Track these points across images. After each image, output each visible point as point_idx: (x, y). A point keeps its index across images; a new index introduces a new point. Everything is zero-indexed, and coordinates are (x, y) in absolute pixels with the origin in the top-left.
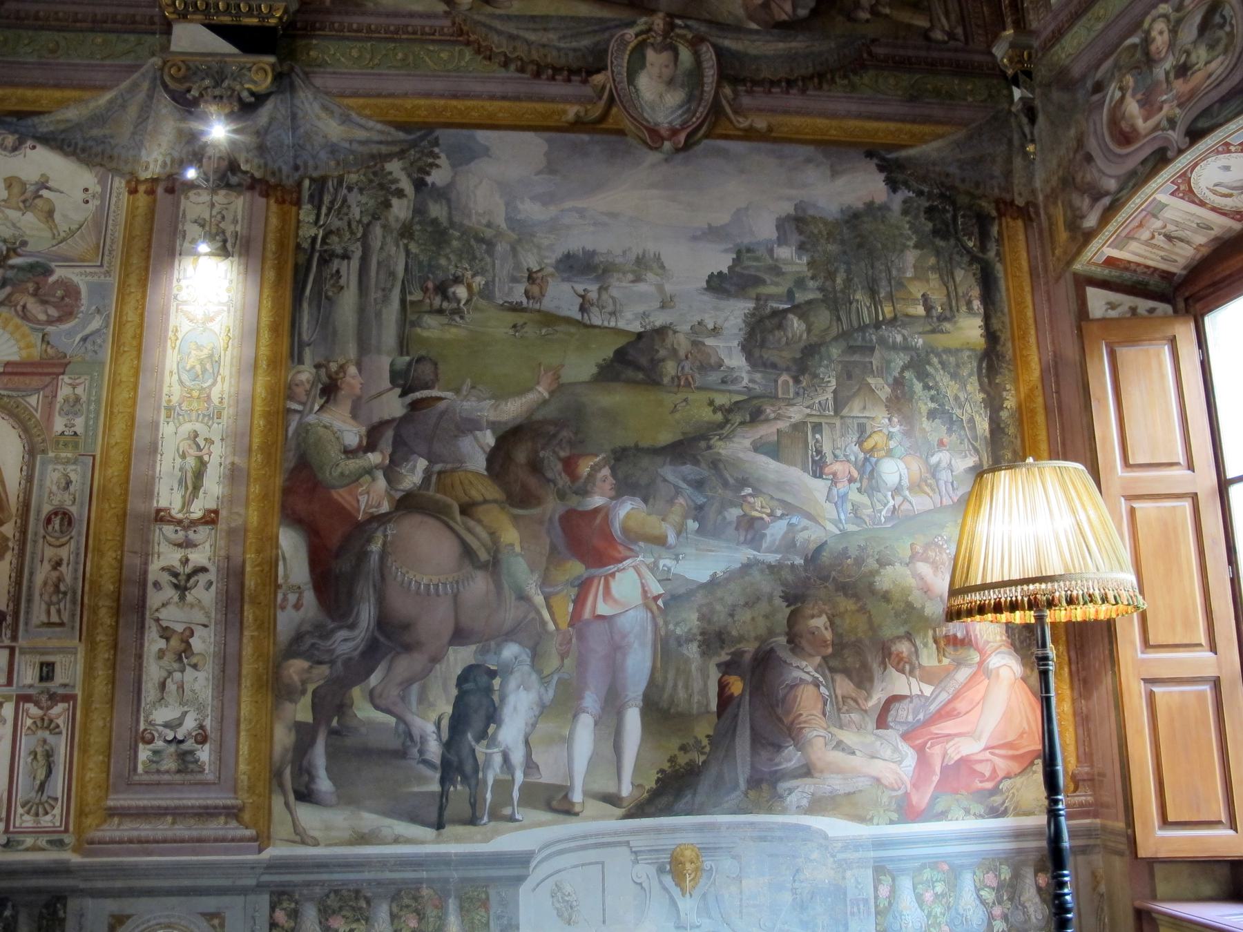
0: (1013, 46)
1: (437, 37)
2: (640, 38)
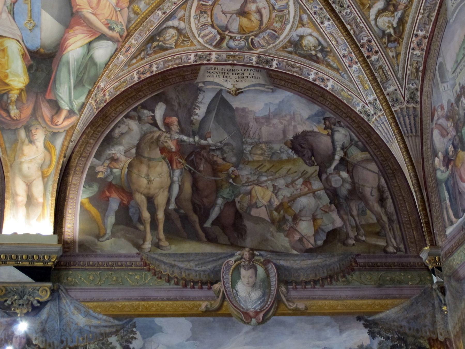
0: (429, 255)
1: (133, 267)
2: (237, 263)
